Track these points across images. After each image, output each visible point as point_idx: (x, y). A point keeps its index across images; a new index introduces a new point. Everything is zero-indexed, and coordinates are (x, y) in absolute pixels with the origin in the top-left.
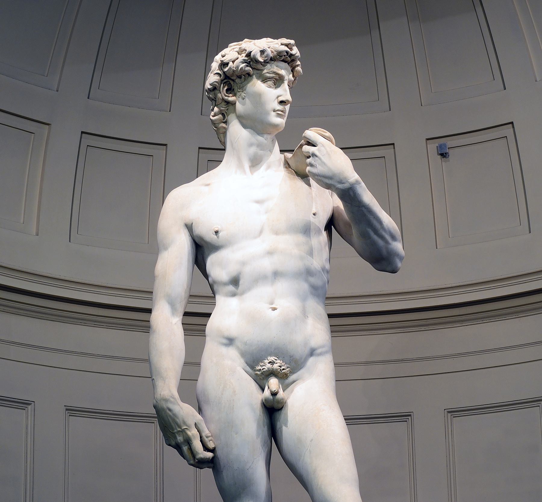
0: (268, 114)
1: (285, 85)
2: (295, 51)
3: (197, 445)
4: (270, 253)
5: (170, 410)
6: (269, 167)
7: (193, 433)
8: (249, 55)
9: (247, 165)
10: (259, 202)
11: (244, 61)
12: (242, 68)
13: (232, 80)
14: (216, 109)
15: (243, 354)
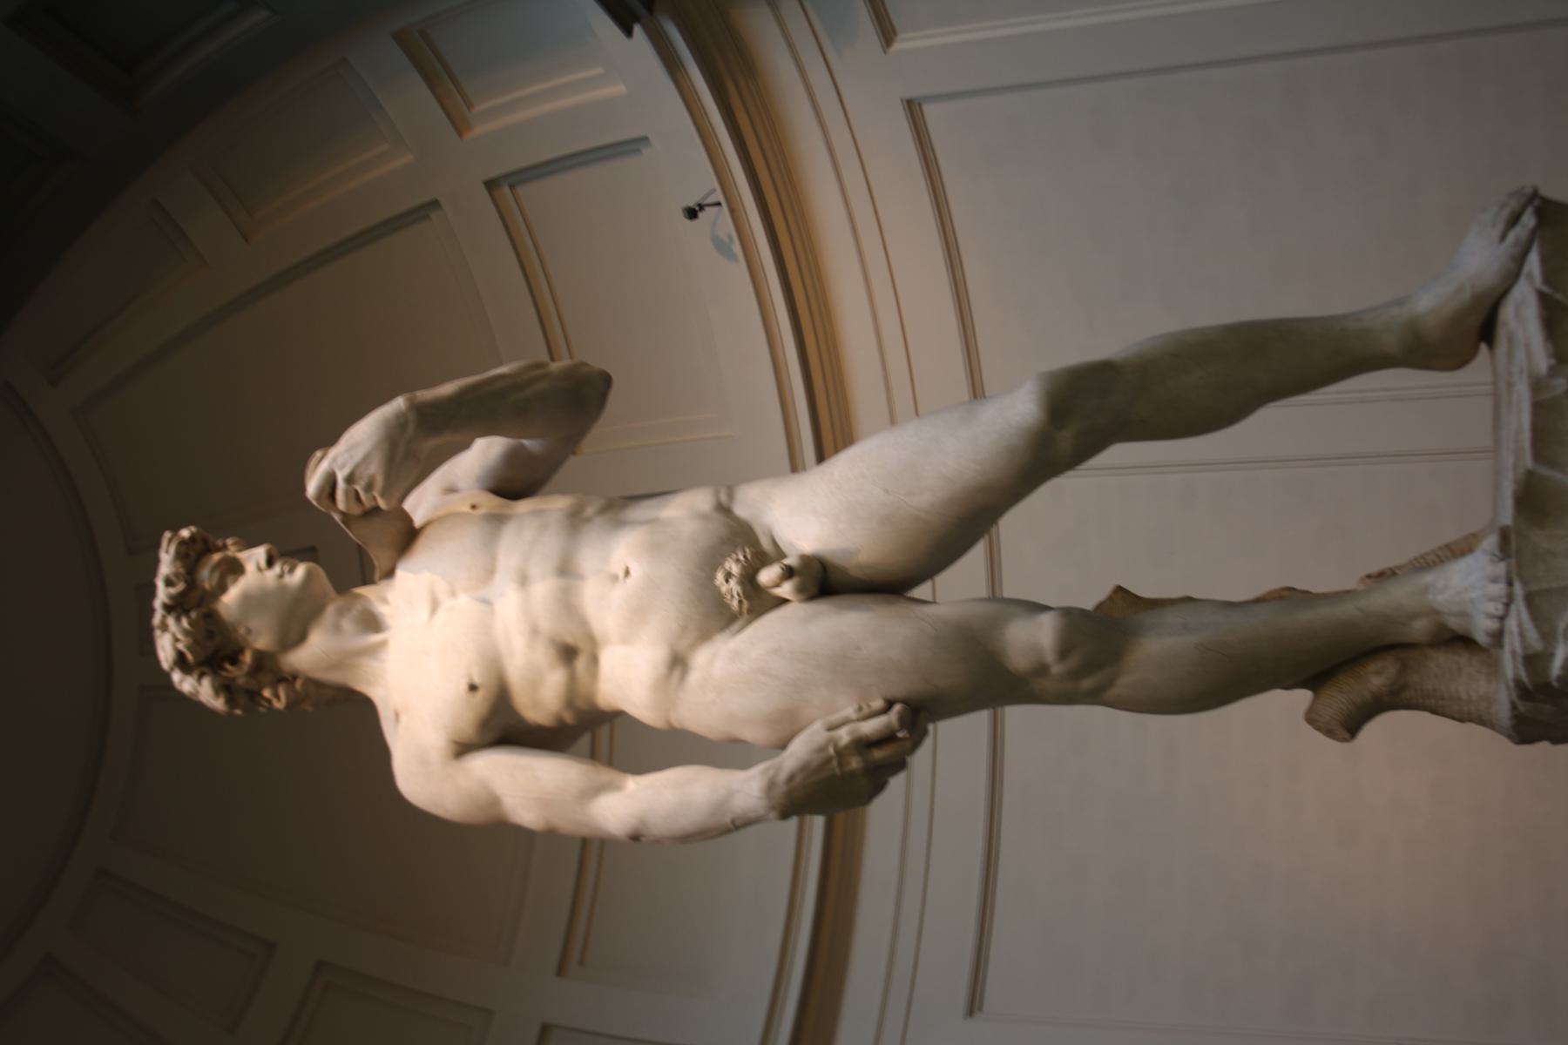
0: (282, 589)
1: (243, 556)
2: (185, 533)
3: (870, 727)
4: (523, 580)
5: (791, 778)
6: (385, 600)
7: (844, 736)
8: (168, 608)
9: (375, 638)
10: (435, 606)
11: (178, 620)
12: (190, 624)
13: (215, 648)
14: (267, 693)
15: (705, 636)
